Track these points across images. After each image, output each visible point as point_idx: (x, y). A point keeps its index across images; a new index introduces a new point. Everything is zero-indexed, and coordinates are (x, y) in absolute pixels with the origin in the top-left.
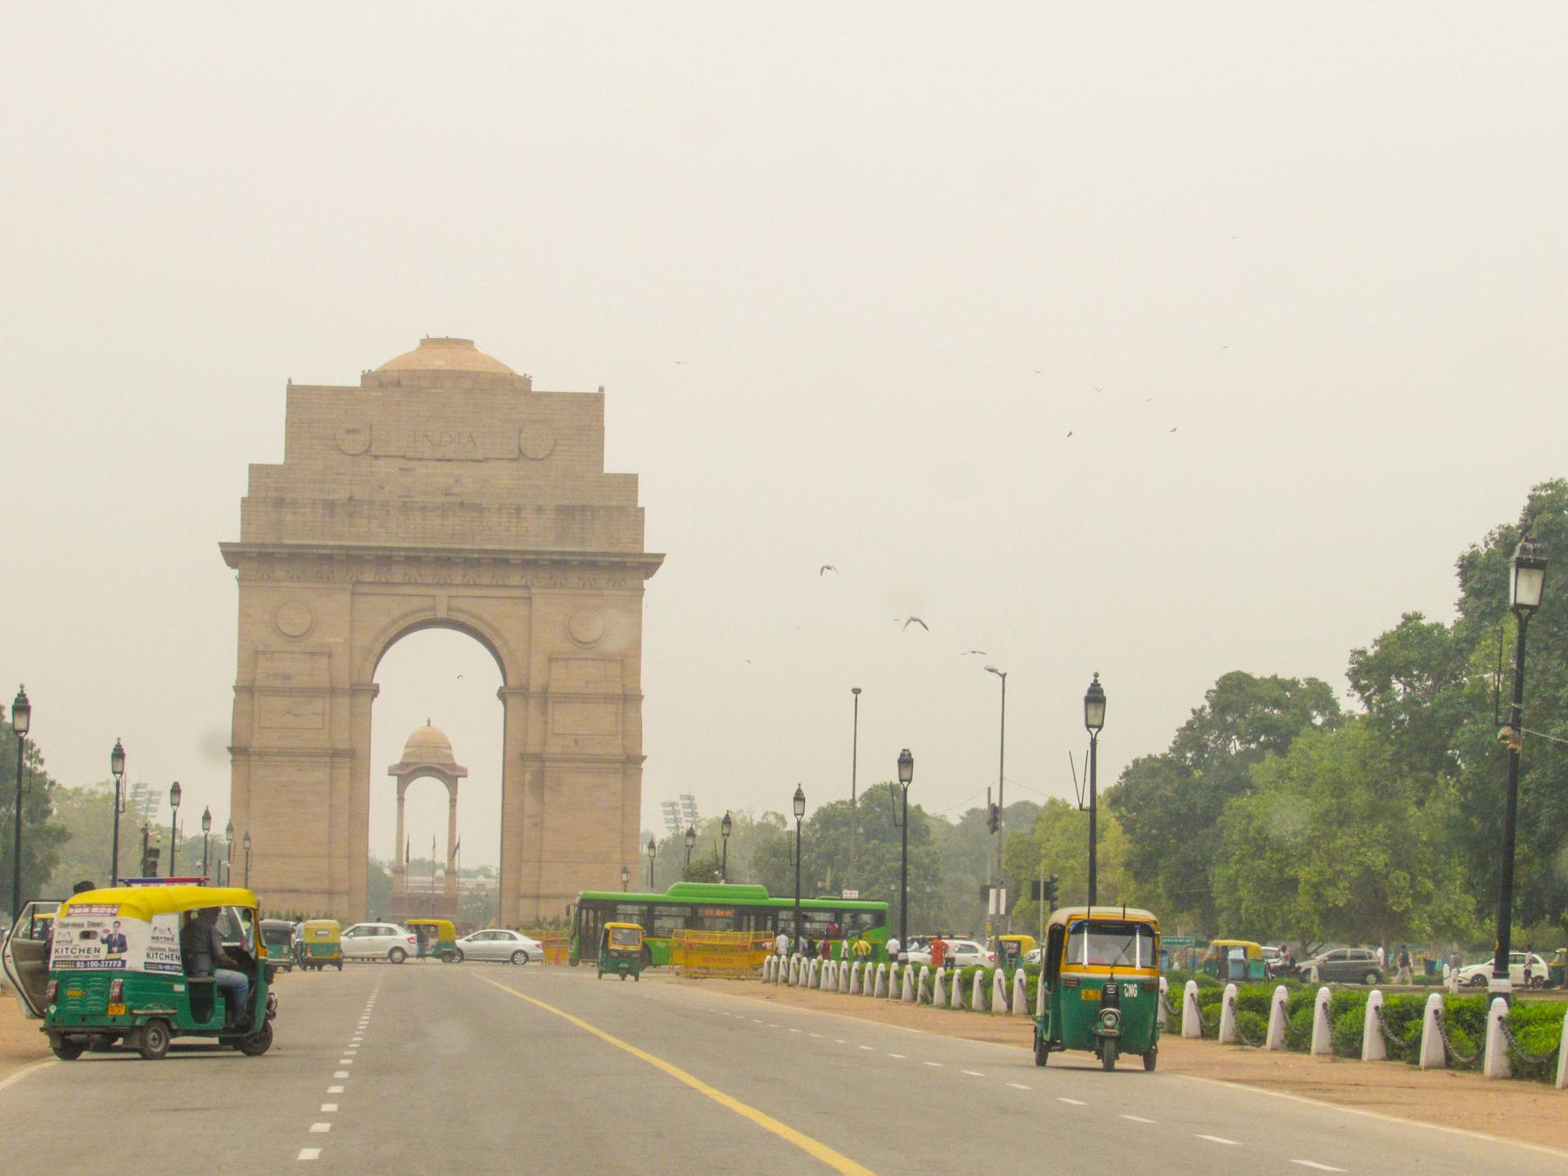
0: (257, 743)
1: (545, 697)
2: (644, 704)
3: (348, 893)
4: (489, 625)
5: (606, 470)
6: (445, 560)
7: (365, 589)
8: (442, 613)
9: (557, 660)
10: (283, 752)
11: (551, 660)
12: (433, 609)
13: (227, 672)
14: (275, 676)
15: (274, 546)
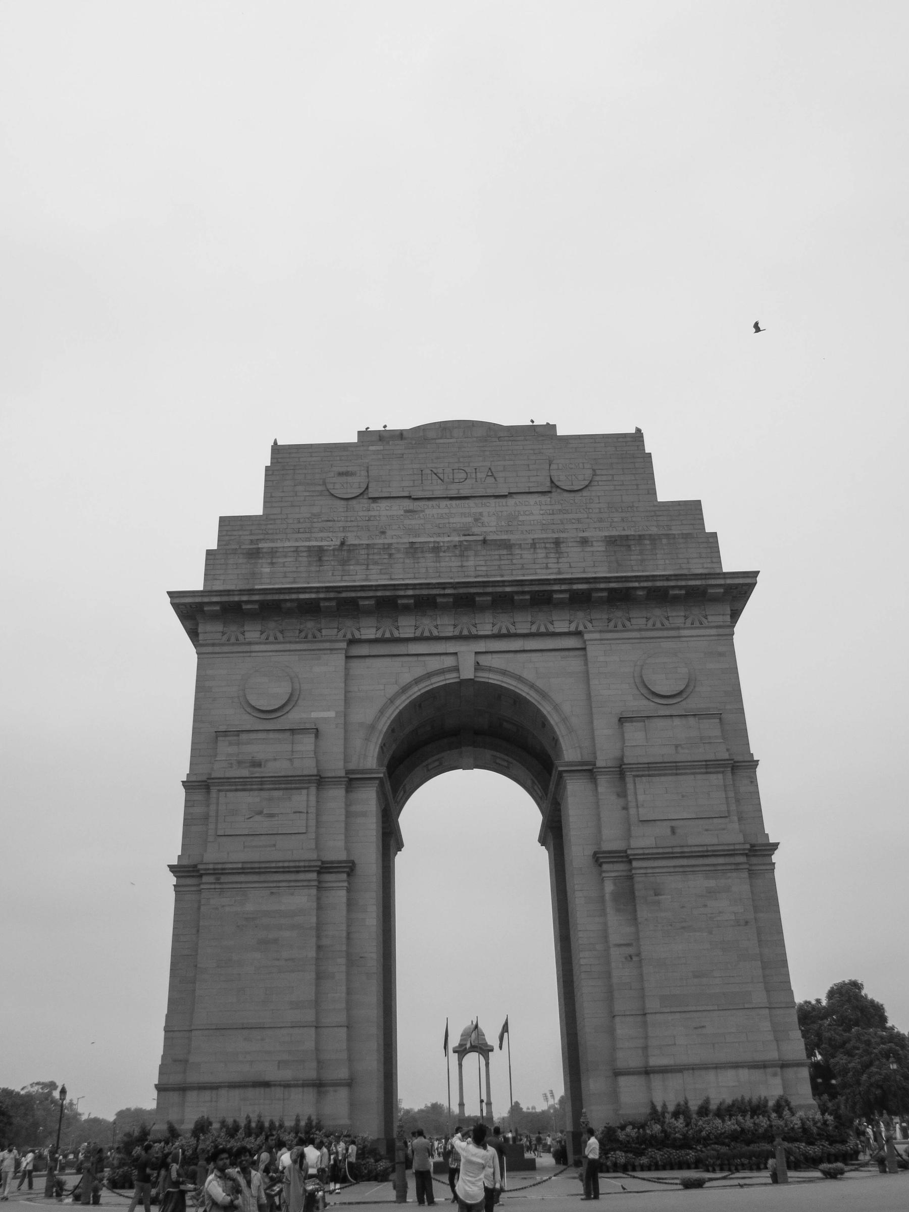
0: (212, 856)
1: (621, 771)
2: (760, 771)
3: (350, 1084)
4: (532, 686)
5: (659, 500)
6: (465, 600)
7: (364, 650)
8: (468, 673)
9: (631, 719)
10: (246, 870)
11: (622, 720)
12: (456, 669)
13: (179, 763)
14: (240, 763)
15: (242, 592)
